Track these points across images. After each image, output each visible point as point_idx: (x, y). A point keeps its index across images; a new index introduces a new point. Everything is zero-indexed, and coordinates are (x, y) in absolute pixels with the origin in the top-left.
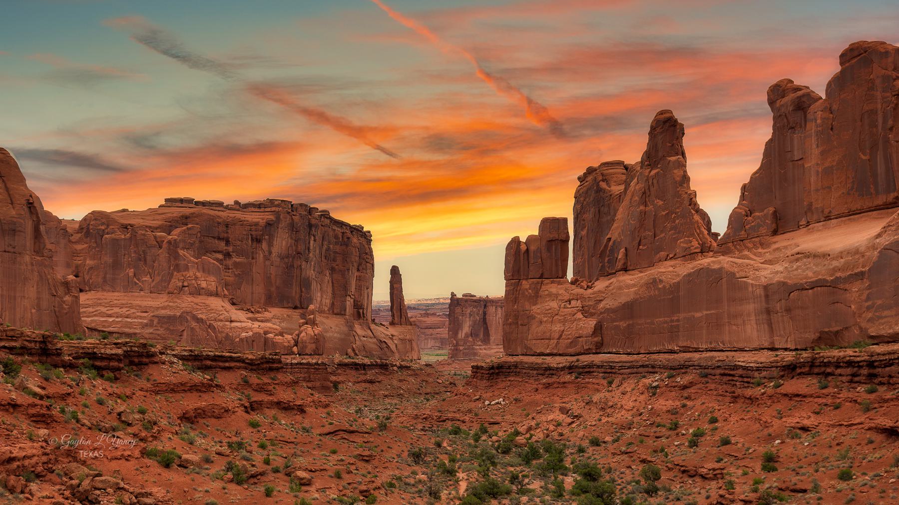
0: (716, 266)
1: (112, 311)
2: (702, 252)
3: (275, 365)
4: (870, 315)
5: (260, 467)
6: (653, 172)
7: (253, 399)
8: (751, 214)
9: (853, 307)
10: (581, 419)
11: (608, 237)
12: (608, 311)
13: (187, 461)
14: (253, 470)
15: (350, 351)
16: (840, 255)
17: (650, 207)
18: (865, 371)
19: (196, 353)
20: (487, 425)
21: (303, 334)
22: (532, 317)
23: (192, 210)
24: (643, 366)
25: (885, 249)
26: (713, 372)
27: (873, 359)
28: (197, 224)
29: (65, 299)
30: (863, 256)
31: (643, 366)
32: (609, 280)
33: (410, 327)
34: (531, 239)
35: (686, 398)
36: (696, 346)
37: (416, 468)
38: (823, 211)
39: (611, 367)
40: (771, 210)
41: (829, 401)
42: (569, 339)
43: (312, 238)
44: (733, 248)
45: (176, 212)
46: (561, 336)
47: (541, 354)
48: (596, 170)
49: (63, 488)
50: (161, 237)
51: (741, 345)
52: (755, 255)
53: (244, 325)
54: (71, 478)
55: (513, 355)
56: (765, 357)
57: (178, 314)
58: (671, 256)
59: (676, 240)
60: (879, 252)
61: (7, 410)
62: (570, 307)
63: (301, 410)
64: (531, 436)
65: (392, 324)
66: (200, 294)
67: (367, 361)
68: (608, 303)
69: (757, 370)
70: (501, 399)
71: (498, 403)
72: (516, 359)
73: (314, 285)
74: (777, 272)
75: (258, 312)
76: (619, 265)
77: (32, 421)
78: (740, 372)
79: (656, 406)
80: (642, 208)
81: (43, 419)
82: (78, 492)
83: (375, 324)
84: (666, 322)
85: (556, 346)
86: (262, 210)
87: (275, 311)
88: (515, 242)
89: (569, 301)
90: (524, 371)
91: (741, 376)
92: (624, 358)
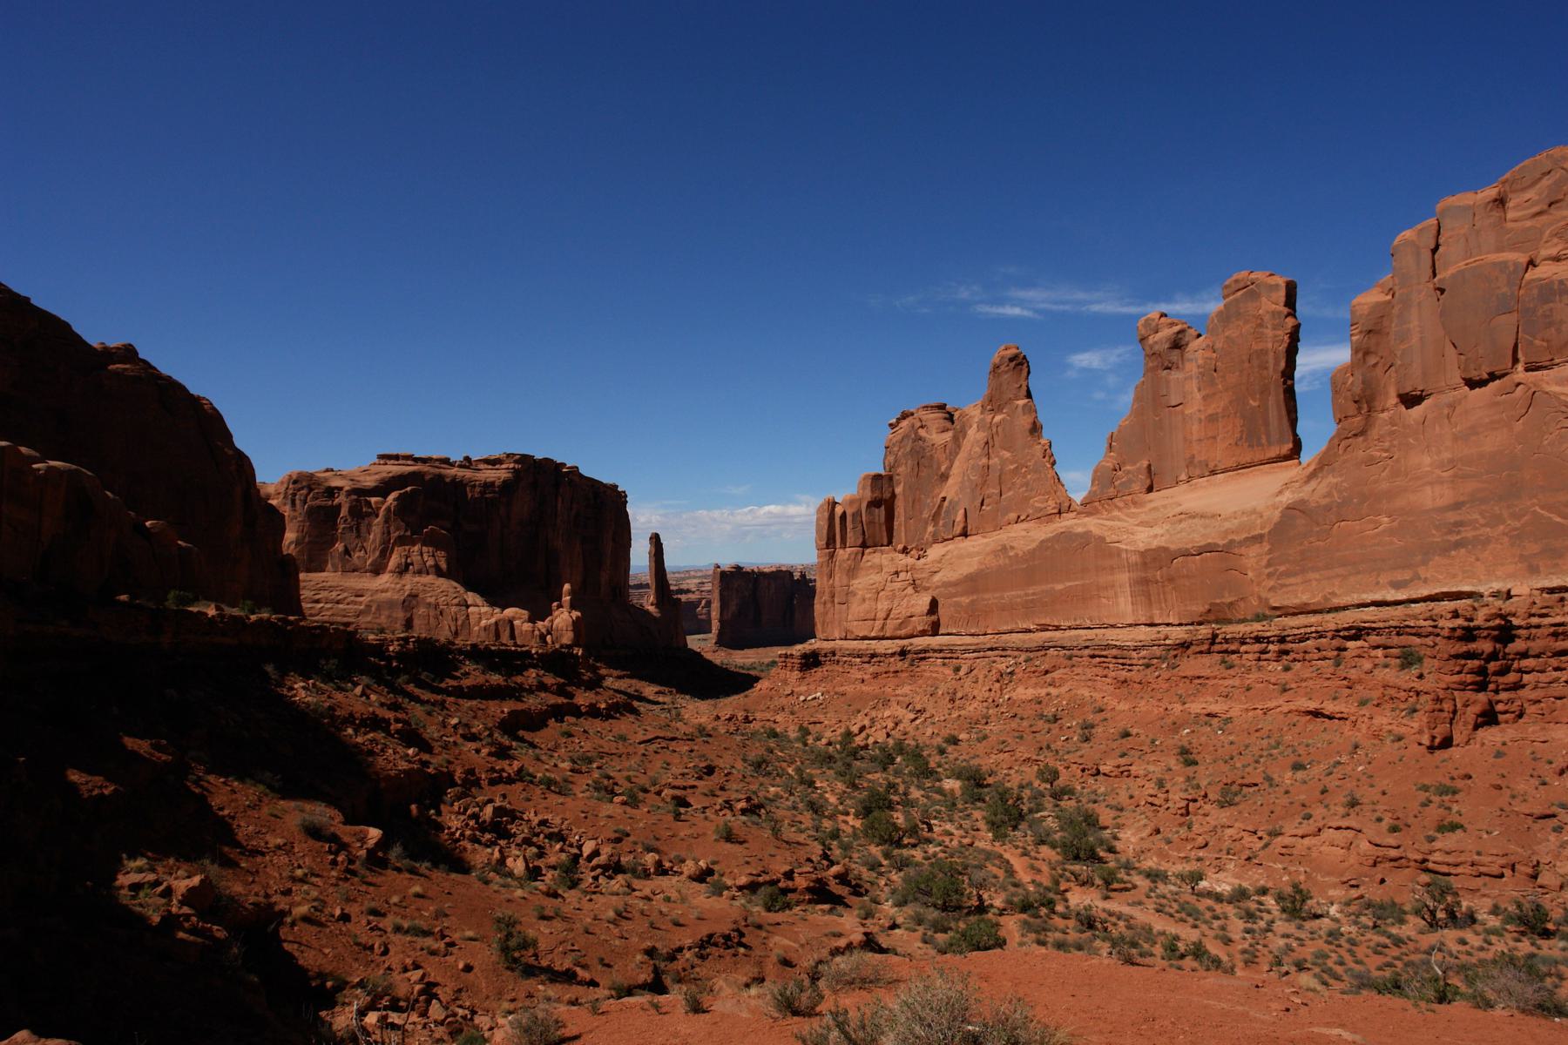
0: (1080, 530)
2: (1060, 513)
4: (1271, 583)
6: (998, 418)
9: (1250, 574)
10: (927, 715)
11: (942, 495)
12: (947, 585)
16: (1234, 516)
17: (995, 461)
20: (805, 725)
24: (991, 649)
25: (1288, 508)
26: (1079, 653)
27: (1286, 633)
30: (1261, 517)
31: (991, 649)
32: (947, 545)
35: (1050, 685)
36: (1056, 624)
38: (1207, 465)
39: (952, 651)
40: (1145, 463)
41: (1236, 682)
43: (560, 499)
44: (1100, 508)
45: (394, 469)
46: (888, 615)
47: (864, 638)
48: (912, 414)
51: (1112, 622)
52: (1128, 516)
56: (1145, 633)
57: (402, 598)
58: (1022, 518)
59: (1027, 499)
60: (1282, 512)
62: (899, 579)
64: (868, 736)
66: (428, 574)
68: (946, 575)
69: (1134, 650)
70: (819, 694)
71: (815, 698)
74: (1156, 536)
76: (958, 529)
78: (1114, 652)
79: (1014, 695)
80: (984, 460)
84: (1019, 596)
85: (883, 628)
89: (897, 573)
90: (845, 659)
91: (1115, 657)
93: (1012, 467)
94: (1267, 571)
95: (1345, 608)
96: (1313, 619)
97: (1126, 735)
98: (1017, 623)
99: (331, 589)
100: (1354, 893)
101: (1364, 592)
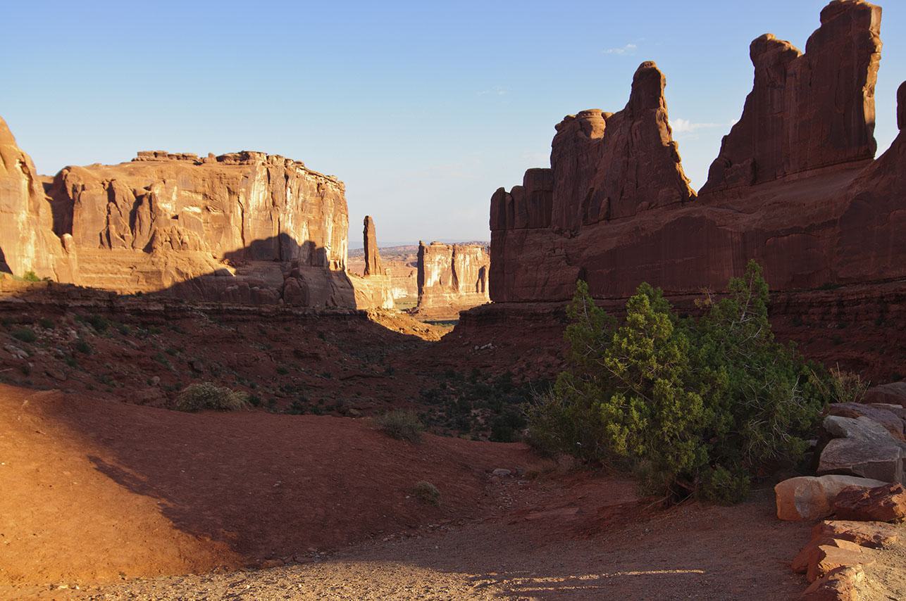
2: (683, 202)
6: (636, 124)
9: (824, 251)
18: (834, 310)
27: (843, 299)
29: (62, 257)
34: (516, 189)
40: (751, 160)
55: (499, 303)
76: (602, 215)
88: (501, 192)
90: (511, 317)
93: (647, 164)
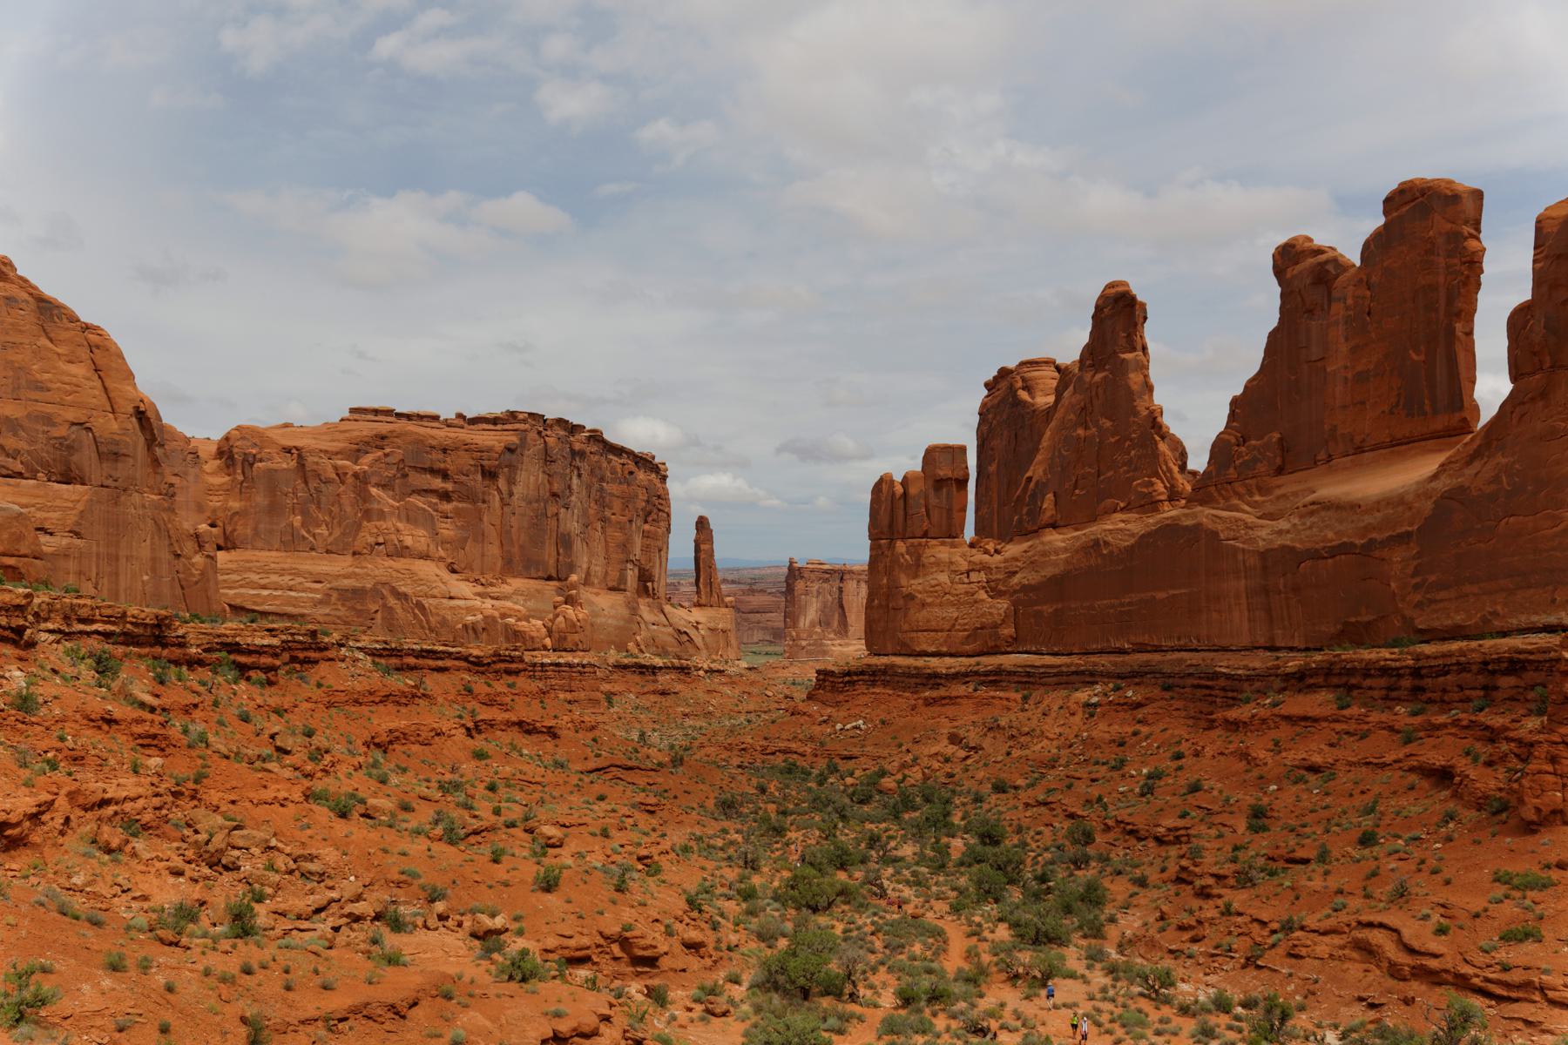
0: (1189, 522)
1: (266, 581)
3: (514, 666)
4: (1418, 597)
5: (488, 818)
6: (1099, 377)
7: (479, 718)
8: (1244, 442)
9: (1393, 585)
11: (1029, 474)
12: (1025, 589)
13: (376, 809)
14: (476, 824)
15: (631, 645)
18: (1407, 683)
19: (393, 646)
21: (561, 619)
22: (910, 597)
23: (389, 427)
24: (1076, 673)
25: (1442, 497)
26: (1181, 682)
27: (1420, 664)
28: (399, 448)
33: (724, 610)
35: (1139, 722)
37: (726, 824)
38: (1352, 440)
39: (1028, 674)
40: (1276, 436)
41: (1352, 727)
42: (965, 630)
44: (1216, 494)
45: (366, 429)
46: (954, 625)
49: (185, 846)
50: (344, 467)
51: (1225, 642)
53: (470, 603)
54: (196, 832)
56: (1259, 661)
57: (369, 586)
58: (1122, 505)
61: (99, 728)
63: (552, 733)
64: (905, 777)
65: (698, 605)
67: (658, 662)
70: (861, 722)
72: (884, 660)
73: (578, 545)
74: (1280, 532)
75: (492, 585)
77: (142, 746)
78: (1222, 682)
79: (1094, 734)
81: (152, 742)
82: (206, 852)
83: (672, 605)
86: (499, 427)
87: (517, 583)
90: (896, 679)
91: (1224, 689)
92: (1049, 660)
93: (1113, 440)
94: (1414, 581)
95: (1504, 634)
96: (1455, 646)
97: (1195, 788)
98: (1108, 641)
99: (282, 572)
100: (1372, 1014)
101: (1536, 613)
